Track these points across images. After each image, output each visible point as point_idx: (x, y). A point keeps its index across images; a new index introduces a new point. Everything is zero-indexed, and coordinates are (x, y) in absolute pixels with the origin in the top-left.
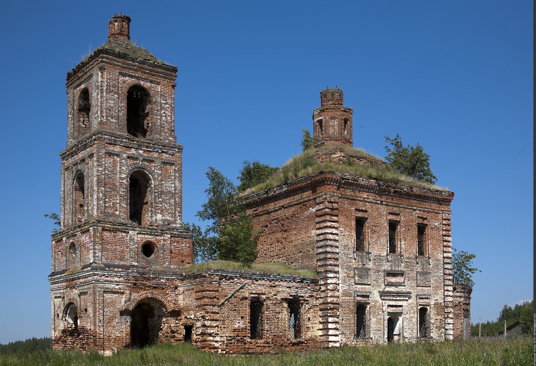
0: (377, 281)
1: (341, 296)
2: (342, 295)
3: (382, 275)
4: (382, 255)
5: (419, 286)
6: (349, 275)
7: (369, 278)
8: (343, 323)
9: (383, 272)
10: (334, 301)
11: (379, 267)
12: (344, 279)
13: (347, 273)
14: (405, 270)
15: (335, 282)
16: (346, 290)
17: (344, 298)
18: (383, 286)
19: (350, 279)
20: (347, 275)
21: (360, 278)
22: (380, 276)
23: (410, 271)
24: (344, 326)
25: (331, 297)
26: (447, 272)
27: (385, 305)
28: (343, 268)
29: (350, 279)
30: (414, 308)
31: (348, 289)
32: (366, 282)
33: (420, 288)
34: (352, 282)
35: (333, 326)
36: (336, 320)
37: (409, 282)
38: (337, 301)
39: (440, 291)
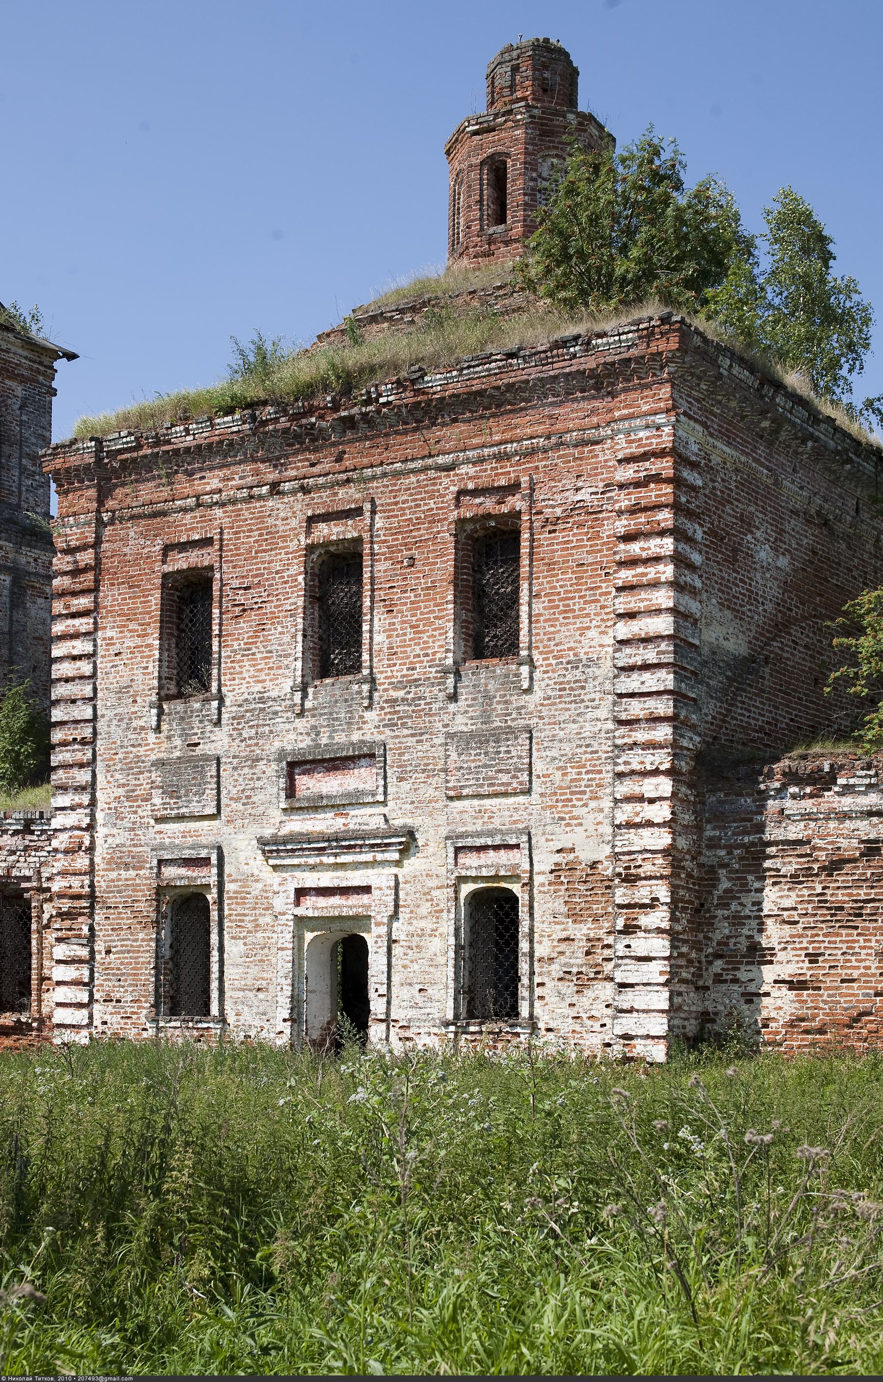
0: (248, 797)
1: (104, 870)
2: (108, 863)
3: (268, 774)
4: (274, 694)
5: (459, 797)
6: (133, 791)
7: (208, 791)
8: (110, 963)
9: (275, 760)
10: (70, 887)
11: (257, 744)
12: (116, 808)
13: (124, 785)
14: (382, 737)
15: (76, 824)
16: (124, 845)
17: (113, 875)
18: (276, 815)
19: (139, 806)
20: (127, 791)
21: (171, 798)
22: (259, 779)
23: (413, 735)
24: (114, 975)
25: (63, 873)
26: (636, 708)
27: (283, 888)
28: (113, 768)
29: (139, 806)
30: (435, 893)
31: (129, 843)
32: (195, 808)
33: (466, 803)
34: (145, 814)
35: (68, 974)
36: (78, 953)
37: (405, 786)
38: (82, 887)
39: (593, 804)
